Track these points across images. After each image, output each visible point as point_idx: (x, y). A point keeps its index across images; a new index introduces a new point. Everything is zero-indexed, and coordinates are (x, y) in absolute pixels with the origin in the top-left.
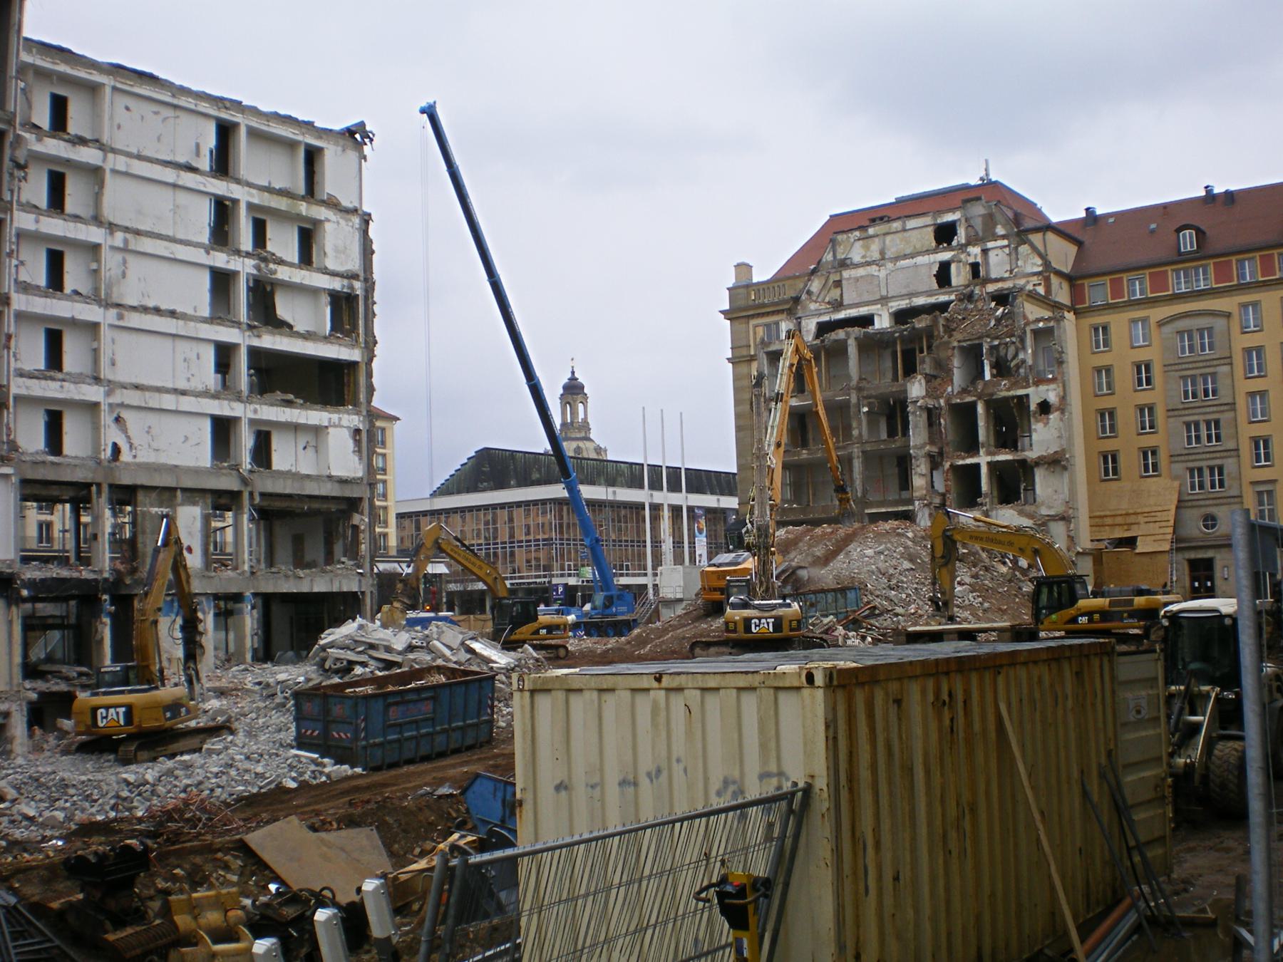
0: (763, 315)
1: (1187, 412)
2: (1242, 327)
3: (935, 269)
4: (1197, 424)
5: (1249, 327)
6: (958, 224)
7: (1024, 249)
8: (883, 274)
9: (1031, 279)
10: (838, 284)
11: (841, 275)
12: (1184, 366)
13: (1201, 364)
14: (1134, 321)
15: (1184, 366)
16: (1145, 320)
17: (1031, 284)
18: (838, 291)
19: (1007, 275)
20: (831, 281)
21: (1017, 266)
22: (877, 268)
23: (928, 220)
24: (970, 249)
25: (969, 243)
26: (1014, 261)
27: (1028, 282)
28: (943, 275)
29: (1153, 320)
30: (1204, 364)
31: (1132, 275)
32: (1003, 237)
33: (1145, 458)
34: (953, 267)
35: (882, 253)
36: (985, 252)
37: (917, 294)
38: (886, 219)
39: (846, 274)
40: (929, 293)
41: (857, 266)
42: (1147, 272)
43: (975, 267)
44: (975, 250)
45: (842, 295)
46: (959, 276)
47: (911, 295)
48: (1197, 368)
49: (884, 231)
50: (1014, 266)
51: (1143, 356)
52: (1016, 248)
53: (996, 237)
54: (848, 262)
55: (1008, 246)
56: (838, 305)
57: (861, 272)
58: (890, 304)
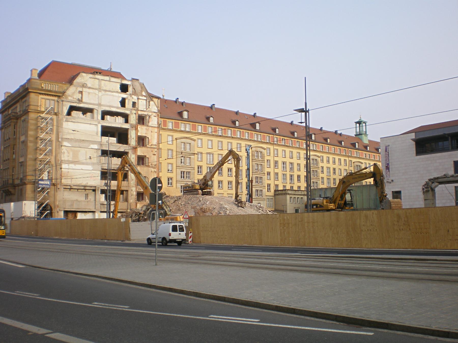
0: (48, 95)
1: (182, 168)
2: (197, 145)
3: (120, 99)
6: (129, 86)
7: (152, 103)
8: (100, 94)
10: (81, 92)
11: (83, 90)
14: (169, 135)
16: (172, 136)
17: (153, 115)
19: (145, 110)
20: (78, 91)
21: (149, 108)
23: (119, 80)
24: (133, 96)
25: (135, 93)
26: (148, 106)
28: (123, 103)
32: (145, 96)
33: (169, 181)
34: (127, 101)
35: (100, 85)
36: (138, 99)
37: (113, 107)
38: (101, 74)
39: (85, 90)
40: (118, 108)
41: (89, 88)
42: (174, 121)
43: (134, 104)
44: (135, 98)
45: (82, 97)
46: (129, 104)
47: (110, 106)
49: (102, 79)
50: (148, 107)
52: (149, 102)
53: (142, 96)
54: (85, 85)
56: (80, 101)
57: (91, 91)
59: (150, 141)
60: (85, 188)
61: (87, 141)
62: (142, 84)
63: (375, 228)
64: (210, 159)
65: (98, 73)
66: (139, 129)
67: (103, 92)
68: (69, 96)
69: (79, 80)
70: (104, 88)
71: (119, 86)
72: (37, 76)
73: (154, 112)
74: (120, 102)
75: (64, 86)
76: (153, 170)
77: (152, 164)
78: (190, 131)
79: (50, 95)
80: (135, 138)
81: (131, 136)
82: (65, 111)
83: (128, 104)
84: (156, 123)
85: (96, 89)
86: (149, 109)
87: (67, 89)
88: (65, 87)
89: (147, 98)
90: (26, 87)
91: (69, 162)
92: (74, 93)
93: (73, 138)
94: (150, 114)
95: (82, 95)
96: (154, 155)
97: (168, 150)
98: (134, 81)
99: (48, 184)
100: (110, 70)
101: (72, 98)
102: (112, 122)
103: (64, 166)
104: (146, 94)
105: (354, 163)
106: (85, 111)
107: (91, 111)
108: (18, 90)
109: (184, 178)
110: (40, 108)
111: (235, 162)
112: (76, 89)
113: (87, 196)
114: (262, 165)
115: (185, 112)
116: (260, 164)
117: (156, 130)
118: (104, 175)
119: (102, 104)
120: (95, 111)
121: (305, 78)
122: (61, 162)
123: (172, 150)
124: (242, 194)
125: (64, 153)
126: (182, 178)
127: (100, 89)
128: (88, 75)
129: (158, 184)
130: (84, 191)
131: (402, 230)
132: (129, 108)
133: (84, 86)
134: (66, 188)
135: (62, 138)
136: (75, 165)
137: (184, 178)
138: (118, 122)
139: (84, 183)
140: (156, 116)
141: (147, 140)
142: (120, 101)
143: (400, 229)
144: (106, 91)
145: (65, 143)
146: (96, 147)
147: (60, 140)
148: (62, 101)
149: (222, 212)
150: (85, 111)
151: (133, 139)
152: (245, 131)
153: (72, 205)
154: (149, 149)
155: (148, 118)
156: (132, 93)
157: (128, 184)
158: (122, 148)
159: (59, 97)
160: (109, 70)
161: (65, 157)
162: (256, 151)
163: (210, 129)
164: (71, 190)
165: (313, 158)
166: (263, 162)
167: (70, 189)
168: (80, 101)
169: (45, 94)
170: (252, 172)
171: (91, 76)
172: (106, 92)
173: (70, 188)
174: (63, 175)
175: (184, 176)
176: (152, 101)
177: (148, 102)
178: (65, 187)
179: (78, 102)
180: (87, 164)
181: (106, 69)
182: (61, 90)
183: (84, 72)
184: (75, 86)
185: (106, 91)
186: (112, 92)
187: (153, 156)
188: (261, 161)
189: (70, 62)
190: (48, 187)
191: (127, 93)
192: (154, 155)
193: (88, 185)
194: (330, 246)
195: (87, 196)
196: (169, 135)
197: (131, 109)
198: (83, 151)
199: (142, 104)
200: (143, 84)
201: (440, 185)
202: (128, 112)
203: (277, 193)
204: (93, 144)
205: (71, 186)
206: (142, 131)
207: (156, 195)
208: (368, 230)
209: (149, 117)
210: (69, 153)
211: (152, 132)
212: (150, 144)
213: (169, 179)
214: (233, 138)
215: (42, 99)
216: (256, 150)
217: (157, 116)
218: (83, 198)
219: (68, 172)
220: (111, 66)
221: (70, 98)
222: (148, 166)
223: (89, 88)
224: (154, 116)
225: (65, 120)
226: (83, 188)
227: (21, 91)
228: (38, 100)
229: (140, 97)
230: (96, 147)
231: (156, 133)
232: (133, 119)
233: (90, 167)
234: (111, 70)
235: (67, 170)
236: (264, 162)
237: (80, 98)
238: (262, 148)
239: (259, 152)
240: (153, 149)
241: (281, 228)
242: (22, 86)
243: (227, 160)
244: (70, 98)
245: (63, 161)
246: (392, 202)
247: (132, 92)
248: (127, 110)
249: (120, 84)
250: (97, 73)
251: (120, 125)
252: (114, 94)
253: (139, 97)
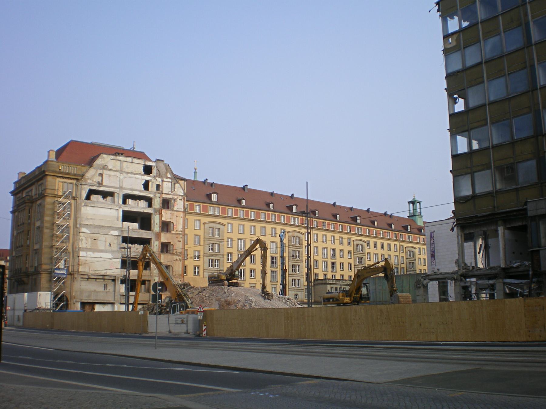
2: (227, 231)
3: (143, 182)
4: (212, 260)
5: (229, 231)
6: (153, 167)
7: (177, 185)
8: (122, 177)
9: (179, 197)
10: (101, 175)
11: (103, 172)
12: (210, 239)
13: (216, 240)
14: (196, 220)
15: (210, 239)
16: (200, 221)
18: (100, 178)
19: (170, 193)
20: (98, 173)
21: (174, 191)
22: (119, 174)
23: (142, 162)
24: (157, 178)
25: (159, 175)
26: (173, 189)
27: (178, 198)
28: (146, 186)
29: (202, 222)
30: (216, 240)
31: (197, 204)
32: (170, 178)
34: (150, 184)
35: (121, 167)
36: (163, 181)
37: (135, 190)
38: (124, 155)
40: (140, 191)
41: (111, 170)
42: (202, 204)
43: (158, 186)
44: (159, 180)
45: (102, 180)
46: (152, 187)
47: (132, 190)
48: (215, 241)
50: (173, 190)
51: (198, 233)
52: (175, 184)
53: (167, 178)
55: (171, 182)
56: (100, 184)
57: (112, 173)
58: (124, 190)
59: (175, 226)
60: (104, 278)
61: (107, 227)
62: (167, 166)
63: (363, 322)
64: (241, 245)
65: (120, 155)
66: (163, 213)
67: (125, 175)
68: (88, 179)
69: (99, 162)
70: (126, 170)
71: (142, 168)
72: (54, 158)
73: (180, 195)
74: (143, 184)
75: (83, 168)
76: (178, 258)
77: (176, 252)
78: (219, 215)
79: (68, 178)
80: (158, 224)
81: (154, 221)
82: (84, 195)
83: (152, 187)
84: (182, 208)
85: (117, 171)
86: (174, 192)
87: (87, 171)
88: (84, 169)
89: (172, 181)
90: (43, 170)
91: (86, 250)
92: (94, 176)
93: (92, 224)
94: (176, 197)
95: (102, 178)
96: (180, 241)
97: (196, 235)
98: (158, 162)
99: (64, 274)
100: (133, 149)
101: (92, 181)
102: (135, 206)
103: (82, 254)
104: (171, 176)
105: (406, 249)
106: (105, 195)
107: (112, 194)
108: (34, 171)
109: (212, 266)
110: (58, 192)
111: (263, 251)
112: (96, 171)
113: (106, 286)
114: (299, 251)
115: (215, 194)
116: (297, 251)
117: (182, 214)
118: (124, 264)
119: (123, 187)
120: (116, 194)
121: (307, 182)
122: (78, 249)
123: (199, 236)
124: (277, 284)
125: (82, 239)
126: (209, 266)
127: (121, 171)
128: (109, 156)
129: (159, 287)
130: (103, 280)
131: (384, 323)
132: (153, 191)
133: (105, 168)
134: (84, 277)
135: (80, 224)
136: (94, 253)
137: (212, 266)
138: (141, 207)
139: (103, 273)
140: (182, 200)
141: (172, 225)
142: (143, 184)
143: (382, 323)
144: (128, 173)
145: (84, 230)
146: (116, 233)
147: (78, 226)
148: (81, 184)
149: (247, 304)
150: (105, 195)
151: (156, 224)
152: (280, 214)
153: (89, 296)
154: (174, 235)
155: (173, 201)
156: (156, 175)
157: (151, 273)
158: (145, 234)
159: (77, 180)
160: (132, 149)
162: (292, 236)
163: (241, 213)
164: (89, 280)
165: (358, 244)
166: (301, 248)
167: (88, 279)
168: (100, 184)
169: (63, 177)
170: (289, 260)
171: (112, 157)
172: (128, 175)
173: (87, 277)
174: (80, 263)
175: (212, 264)
176: (178, 183)
177: (173, 185)
178: (82, 276)
179: (98, 185)
180: (106, 252)
181: (129, 149)
182: (80, 173)
183: (105, 154)
184: (94, 168)
185: (128, 173)
186: (135, 174)
187: (178, 243)
188: (299, 248)
189: (89, 141)
190: (65, 276)
191: (151, 175)
192: (180, 241)
193: (107, 274)
194: (326, 338)
195: (106, 286)
196: (196, 220)
197: (155, 193)
198: (102, 238)
199: (167, 187)
200: (168, 165)
201: (431, 282)
202: (151, 195)
203: (317, 282)
204: (113, 230)
205: (89, 276)
206: (167, 215)
207: (156, 296)
208: (357, 323)
209: (175, 200)
210: (87, 240)
211: (177, 217)
212: (175, 230)
213: (195, 268)
214: (266, 222)
215: (59, 183)
216: (293, 235)
217: (183, 200)
218: (101, 289)
219: (86, 260)
220: (134, 145)
221: (89, 181)
222: (173, 254)
223: (111, 170)
224: (180, 200)
225: (83, 204)
226: (101, 277)
227: (37, 173)
228: (55, 183)
229: (165, 179)
230: (116, 233)
231: (182, 218)
232: (157, 203)
233: (109, 255)
234: (135, 150)
235: (85, 258)
236: (302, 248)
237: (100, 181)
238: (299, 232)
239: (297, 237)
240: (178, 236)
241: (285, 321)
242: (38, 168)
243: (254, 249)
244: (89, 181)
245: (81, 249)
246: (400, 296)
247: (157, 174)
248: (151, 193)
249: (143, 165)
250: (119, 154)
251: (143, 209)
252: (137, 176)
253: (164, 179)
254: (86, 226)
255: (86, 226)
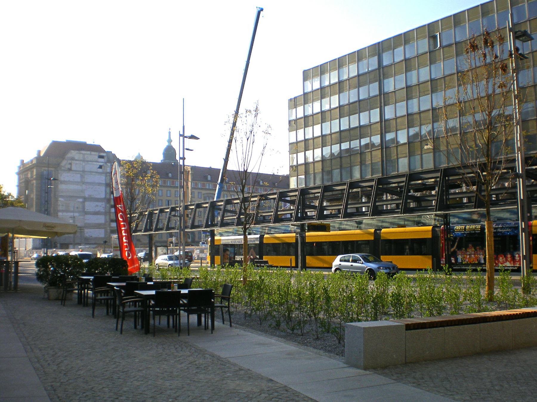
8: (84, 164)
10: (71, 164)
18: (70, 166)
41: (76, 160)
45: (71, 167)
57: (77, 162)
69: (69, 155)
91: (63, 211)
127: (84, 161)
133: (73, 159)
144: (88, 161)
145: (60, 199)
161: (60, 208)
171: (77, 152)
183: (74, 150)
221: (63, 168)
223: (76, 160)
244: (63, 168)
247: (107, 160)
254: (62, 197)
255: (62, 197)
